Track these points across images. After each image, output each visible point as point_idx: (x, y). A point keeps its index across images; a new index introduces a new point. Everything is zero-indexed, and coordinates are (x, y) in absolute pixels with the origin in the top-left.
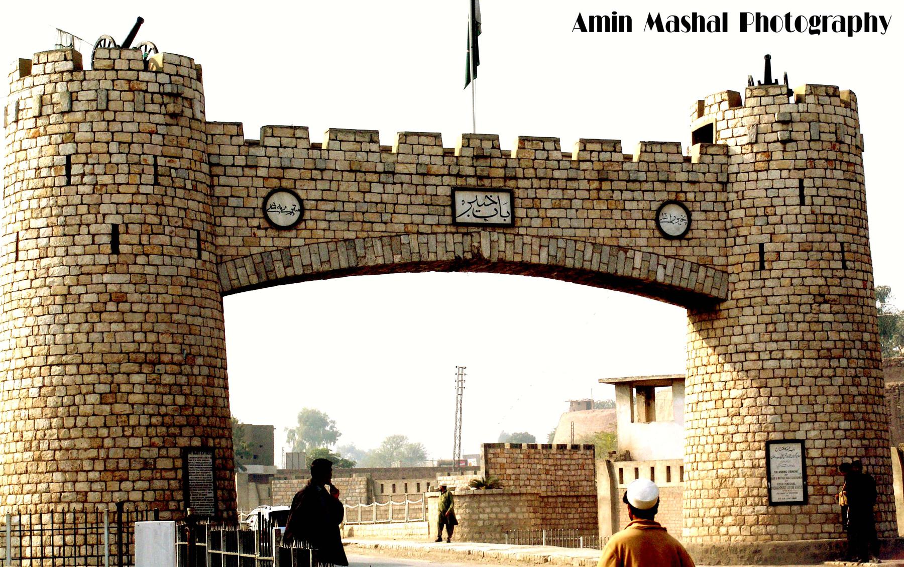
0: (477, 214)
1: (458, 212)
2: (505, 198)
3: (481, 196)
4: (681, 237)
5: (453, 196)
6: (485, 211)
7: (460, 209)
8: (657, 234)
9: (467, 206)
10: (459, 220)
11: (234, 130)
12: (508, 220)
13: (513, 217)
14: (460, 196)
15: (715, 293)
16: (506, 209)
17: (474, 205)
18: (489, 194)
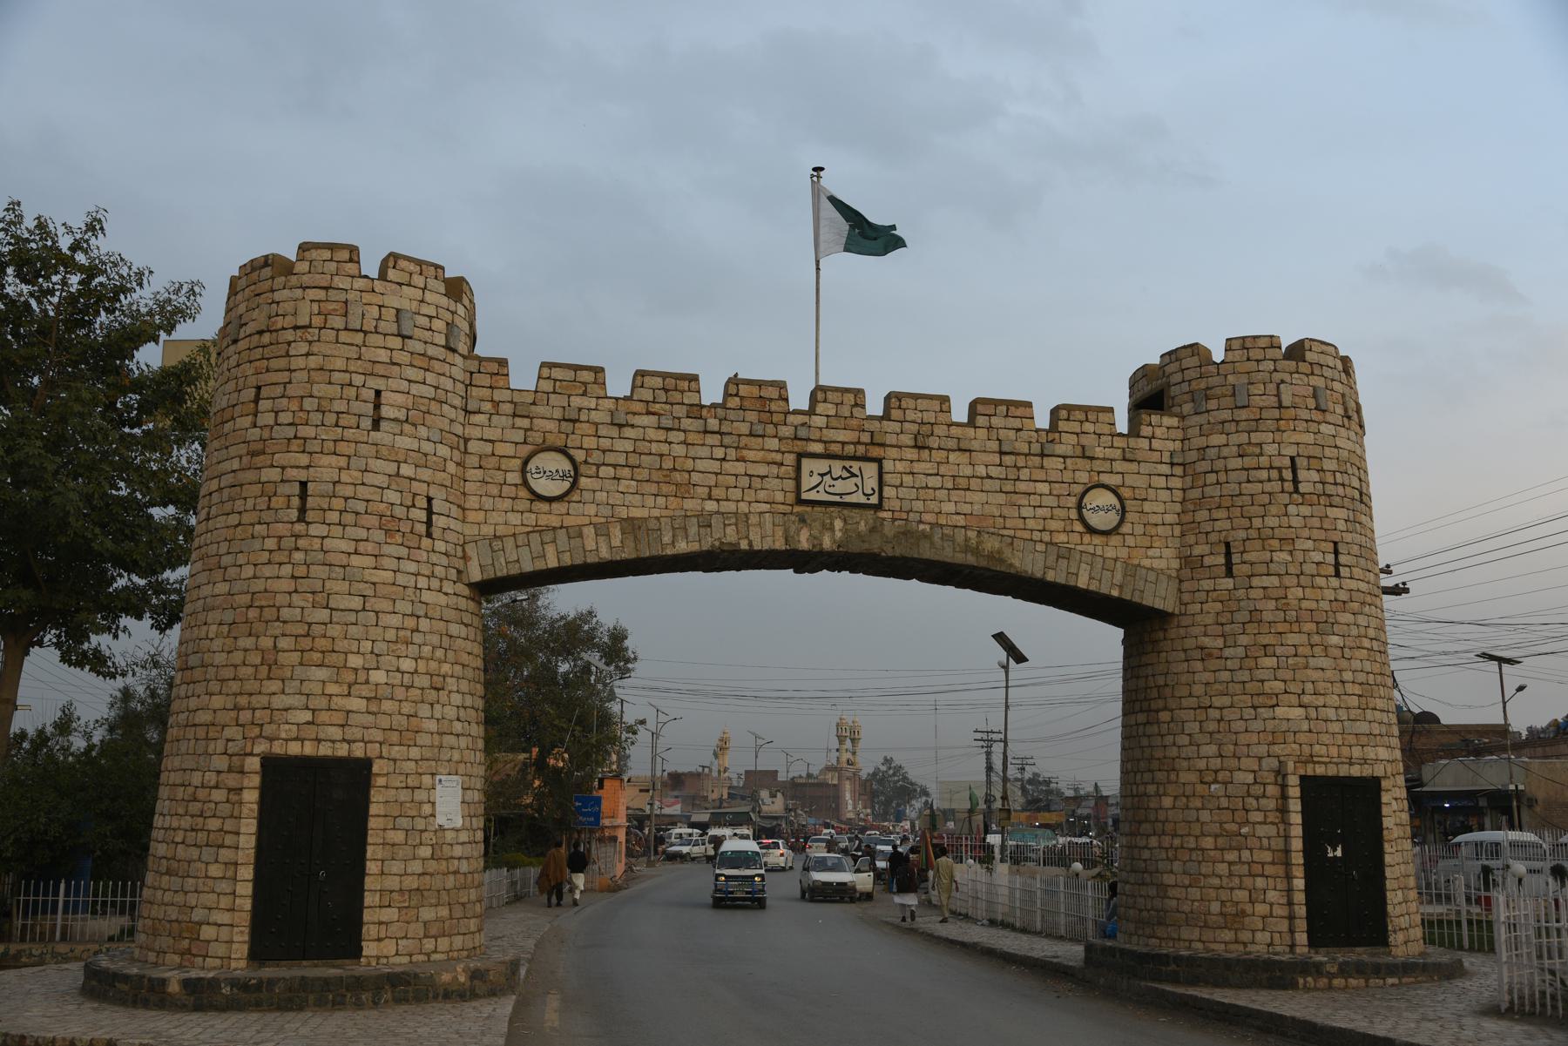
0: (831, 490)
1: (804, 487)
2: (870, 470)
3: (837, 467)
4: (1115, 531)
5: (798, 468)
6: (840, 486)
7: (807, 482)
8: (1078, 527)
9: (816, 479)
10: (805, 496)
11: (494, 367)
12: (874, 500)
13: (881, 497)
14: (805, 462)
15: (1159, 604)
16: (871, 483)
17: (827, 478)
18: (847, 464)
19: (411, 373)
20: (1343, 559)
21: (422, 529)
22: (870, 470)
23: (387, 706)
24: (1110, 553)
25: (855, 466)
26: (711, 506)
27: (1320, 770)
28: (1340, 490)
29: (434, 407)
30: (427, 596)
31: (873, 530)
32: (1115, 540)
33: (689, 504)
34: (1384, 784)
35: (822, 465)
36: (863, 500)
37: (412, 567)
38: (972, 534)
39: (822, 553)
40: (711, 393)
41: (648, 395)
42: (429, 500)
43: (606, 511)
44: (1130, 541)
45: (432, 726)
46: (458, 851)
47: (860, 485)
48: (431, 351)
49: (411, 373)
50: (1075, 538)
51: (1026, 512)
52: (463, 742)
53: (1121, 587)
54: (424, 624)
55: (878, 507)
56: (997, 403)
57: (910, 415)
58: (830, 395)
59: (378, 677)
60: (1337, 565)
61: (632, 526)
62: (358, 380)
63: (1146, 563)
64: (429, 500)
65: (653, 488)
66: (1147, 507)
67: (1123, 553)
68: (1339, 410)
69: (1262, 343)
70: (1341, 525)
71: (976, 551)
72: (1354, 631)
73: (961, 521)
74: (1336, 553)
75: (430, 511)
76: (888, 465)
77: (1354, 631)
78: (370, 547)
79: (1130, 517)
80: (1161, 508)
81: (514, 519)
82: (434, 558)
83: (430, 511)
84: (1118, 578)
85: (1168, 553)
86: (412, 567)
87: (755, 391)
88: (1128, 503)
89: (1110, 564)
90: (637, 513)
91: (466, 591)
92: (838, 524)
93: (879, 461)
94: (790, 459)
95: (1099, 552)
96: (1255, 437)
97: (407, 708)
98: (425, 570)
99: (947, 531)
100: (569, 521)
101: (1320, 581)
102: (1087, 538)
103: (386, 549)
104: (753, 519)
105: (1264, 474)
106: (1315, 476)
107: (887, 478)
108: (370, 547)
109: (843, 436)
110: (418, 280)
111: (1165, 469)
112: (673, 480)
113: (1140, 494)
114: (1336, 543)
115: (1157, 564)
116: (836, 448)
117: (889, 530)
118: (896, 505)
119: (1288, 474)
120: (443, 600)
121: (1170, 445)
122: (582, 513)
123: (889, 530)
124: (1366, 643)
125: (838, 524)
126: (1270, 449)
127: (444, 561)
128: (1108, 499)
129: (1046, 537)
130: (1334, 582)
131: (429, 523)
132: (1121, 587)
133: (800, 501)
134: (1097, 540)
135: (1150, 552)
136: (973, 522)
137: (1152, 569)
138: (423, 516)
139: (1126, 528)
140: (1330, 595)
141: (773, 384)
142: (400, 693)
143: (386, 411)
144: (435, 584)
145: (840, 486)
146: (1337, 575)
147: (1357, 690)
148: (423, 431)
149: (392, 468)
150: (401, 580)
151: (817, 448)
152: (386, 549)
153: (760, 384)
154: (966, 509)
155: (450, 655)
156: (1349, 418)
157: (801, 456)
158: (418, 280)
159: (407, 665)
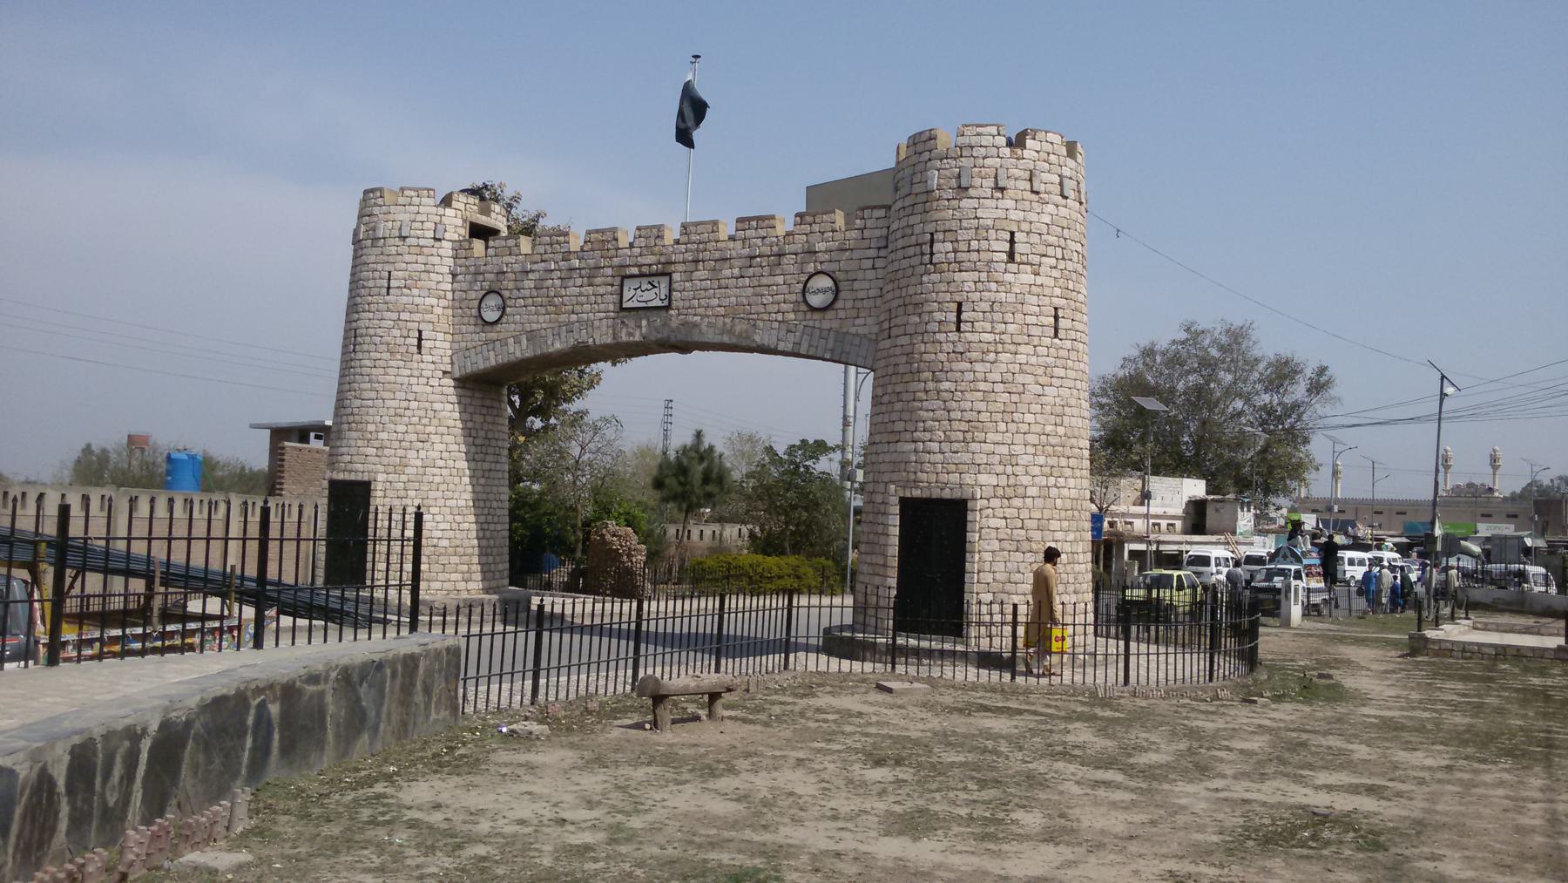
7: (627, 294)
12: (666, 303)
19: (408, 258)
20: (964, 316)
21: (415, 349)
22: (664, 282)
23: (387, 451)
24: (826, 325)
25: (655, 280)
26: (574, 317)
27: (917, 493)
28: (974, 256)
29: (423, 276)
30: (415, 388)
31: (665, 324)
32: (830, 314)
33: (563, 318)
34: (970, 505)
35: (635, 283)
36: (660, 304)
37: (408, 372)
38: (728, 320)
39: (636, 344)
40: (575, 244)
41: (541, 249)
42: (420, 332)
43: (519, 327)
44: (842, 314)
45: (419, 463)
46: (439, 534)
47: (653, 296)
48: (422, 242)
49: (408, 258)
50: (801, 316)
51: (767, 299)
52: (445, 472)
53: (832, 350)
54: (414, 405)
55: (668, 308)
56: (749, 219)
57: (694, 238)
58: (643, 233)
59: (384, 436)
60: (959, 321)
61: (532, 335)
62: (379, 267)
63: (853, 330)
64: (420, 332)
65: (543, 310)
66: (856, 285)
67: (835, 324)
68: (990, 183)
69: (924, 138)
70: (969, 286)
71: (730, 332)
72: (969, 376)
73: (722, 311)
74: (959, 312)
75: (420, 339)
76: (676, 277)
77: (969, 376)
78: (382, 363)
79: (842, 295)
80: (866, 285)
81: (476, 337)
82: (422, 366)
83: (420, 339)
84: (831, 344)
85: (870, 321)
86: (408, 372)
87: (599, 236)
88: (841, 285)
89: (825, 334)
90: (535, 326)
91: (452, 383)
92: (644, 323)
93: (670, 274)
94: (617, 281)
95: (817, 325)
96: (912, 220)
97: (400, 452)
98: (416, 373)
99: (713, 320)
100: (501, 336)
101: (941, 337)
102: (809, 315)
103: (392, 363)
104: (597, 323)
105: (911, 251)
106: (949, 246)
107: (675, 286)
108: (382, 363)
109: (651, 259)
110: (416, 200)
111: (873, 253)
112: (552, 305)
113: (852, 276)
114: (960, 305)
115: (861, 331)
116: (645, 270)
117: (674, 323)
118: (681, 304)
119: (926, 249)
120: (429, 389)
121: (878, 233)
122: (506, 329)
123: (674, 323)
124: (982, 386)
125: (644, 323)
126: (918, 229)
127: (432, 367)
128: (825, 282)
129: (780, 318)
130: (953, 336)
131: (419, 346)
132: (832, 350)
133: (622, 309)
134: (817, 316)
135: (857, 322)
136: (730, 310)
137: (857, 335)
138: (415, 342)
139: (839, 304)
140: (948, 347)
141: (610, 230)
142: (396, 444)
143: (393, 283)
144: (423, 380)
145: (647, 296)
146: (958, 329)
147: (964, 426)
148: (415, 292)
149: (395, 316)
150: (399, 379)
151: (635, 271)
152: (392, 363)
153: (602, 231)
154: (726, 302)
155: (435, 422)
156: (1002, 190)
157: (624, 277)
158: (416, 200)
159: (401, 428)
